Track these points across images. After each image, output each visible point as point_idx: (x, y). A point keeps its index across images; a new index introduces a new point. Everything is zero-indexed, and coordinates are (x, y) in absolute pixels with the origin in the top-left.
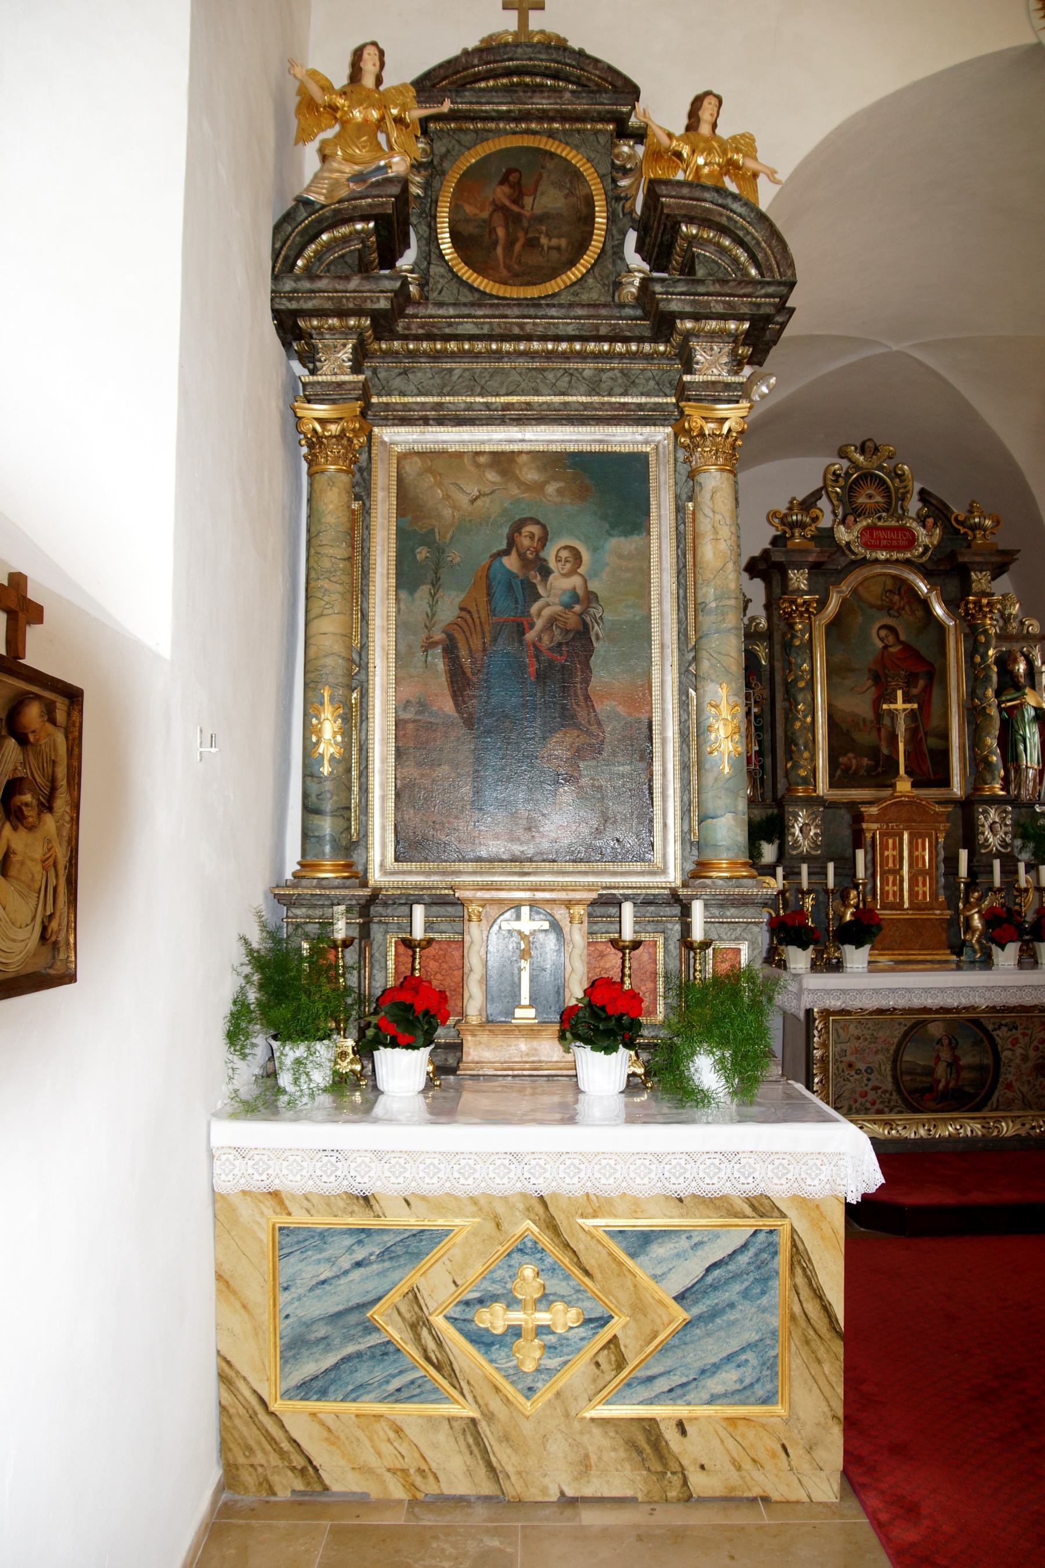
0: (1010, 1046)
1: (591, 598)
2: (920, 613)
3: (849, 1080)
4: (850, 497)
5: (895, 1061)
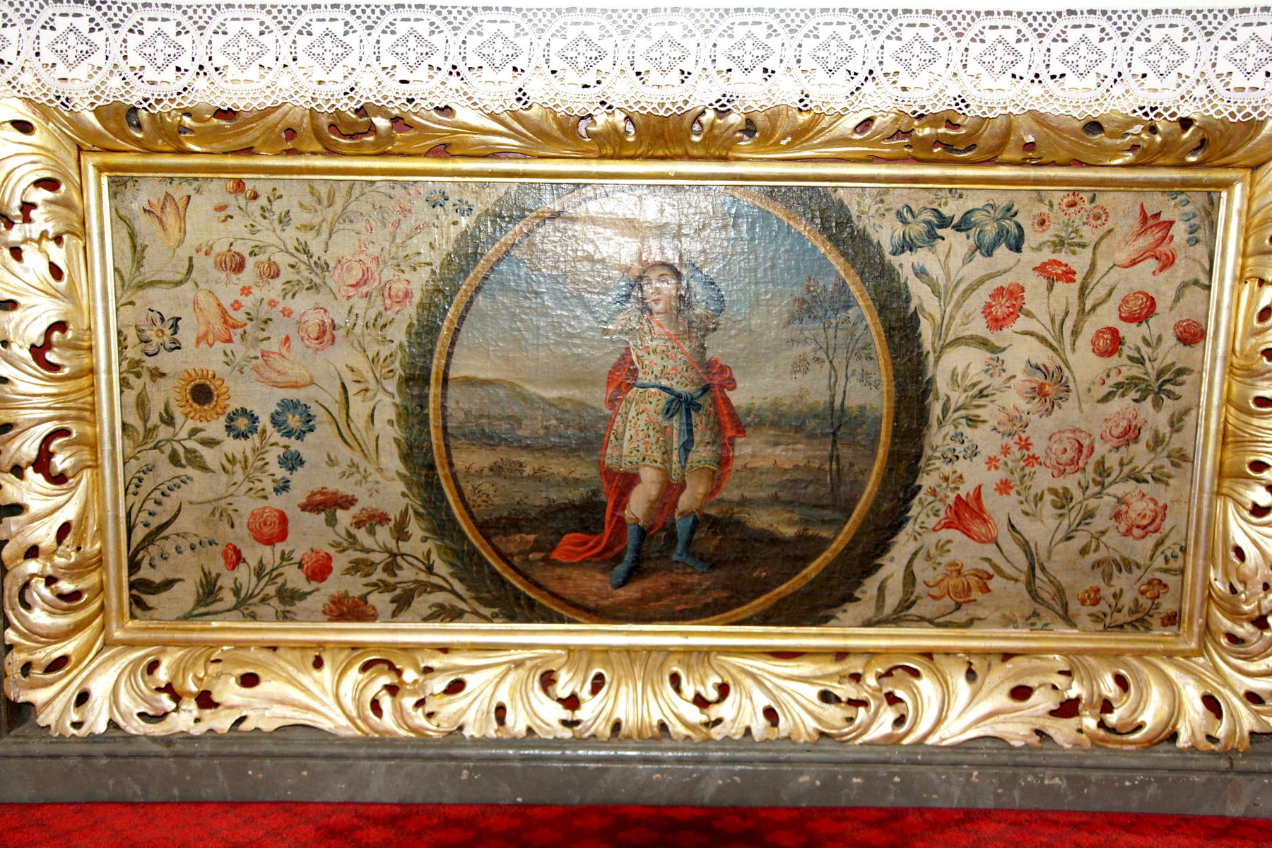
0: (979, 327)
3: (196, 461)
5: (416, 379)
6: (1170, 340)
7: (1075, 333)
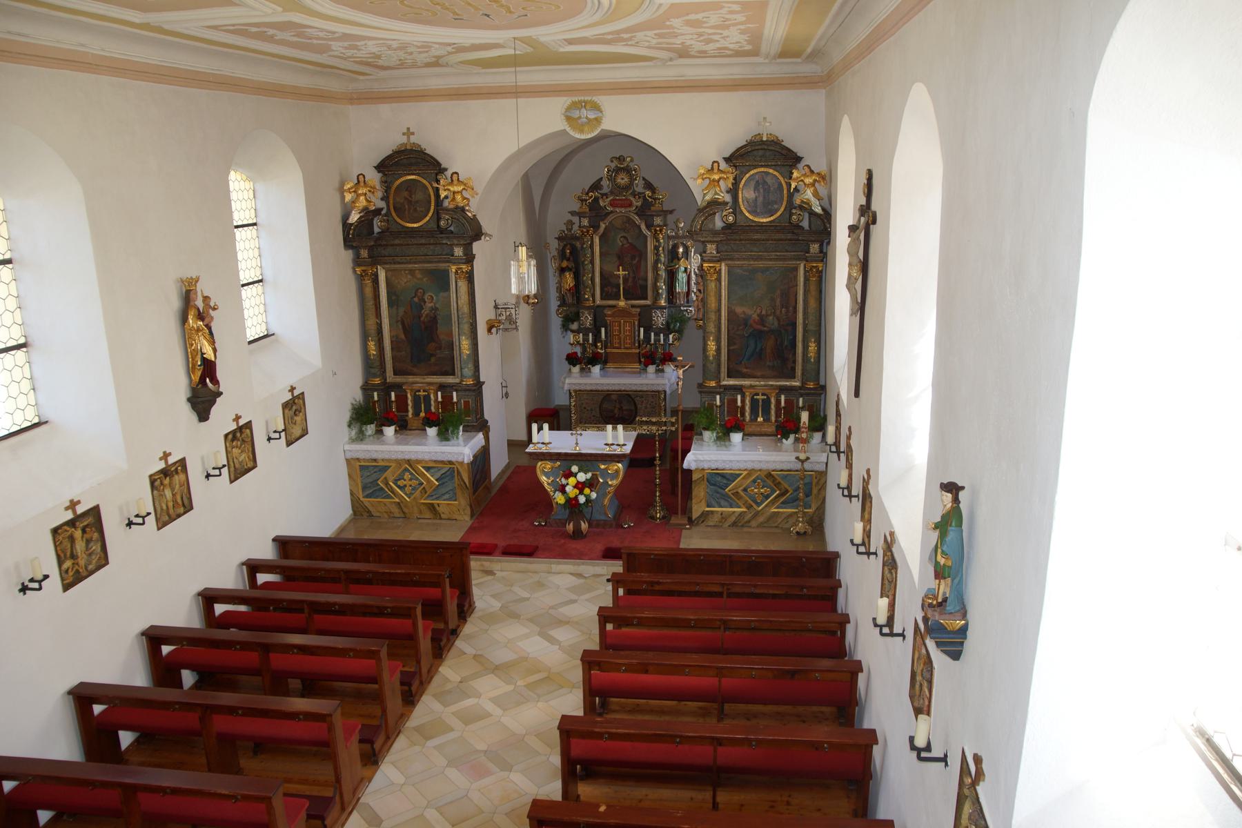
1: (436, 309)
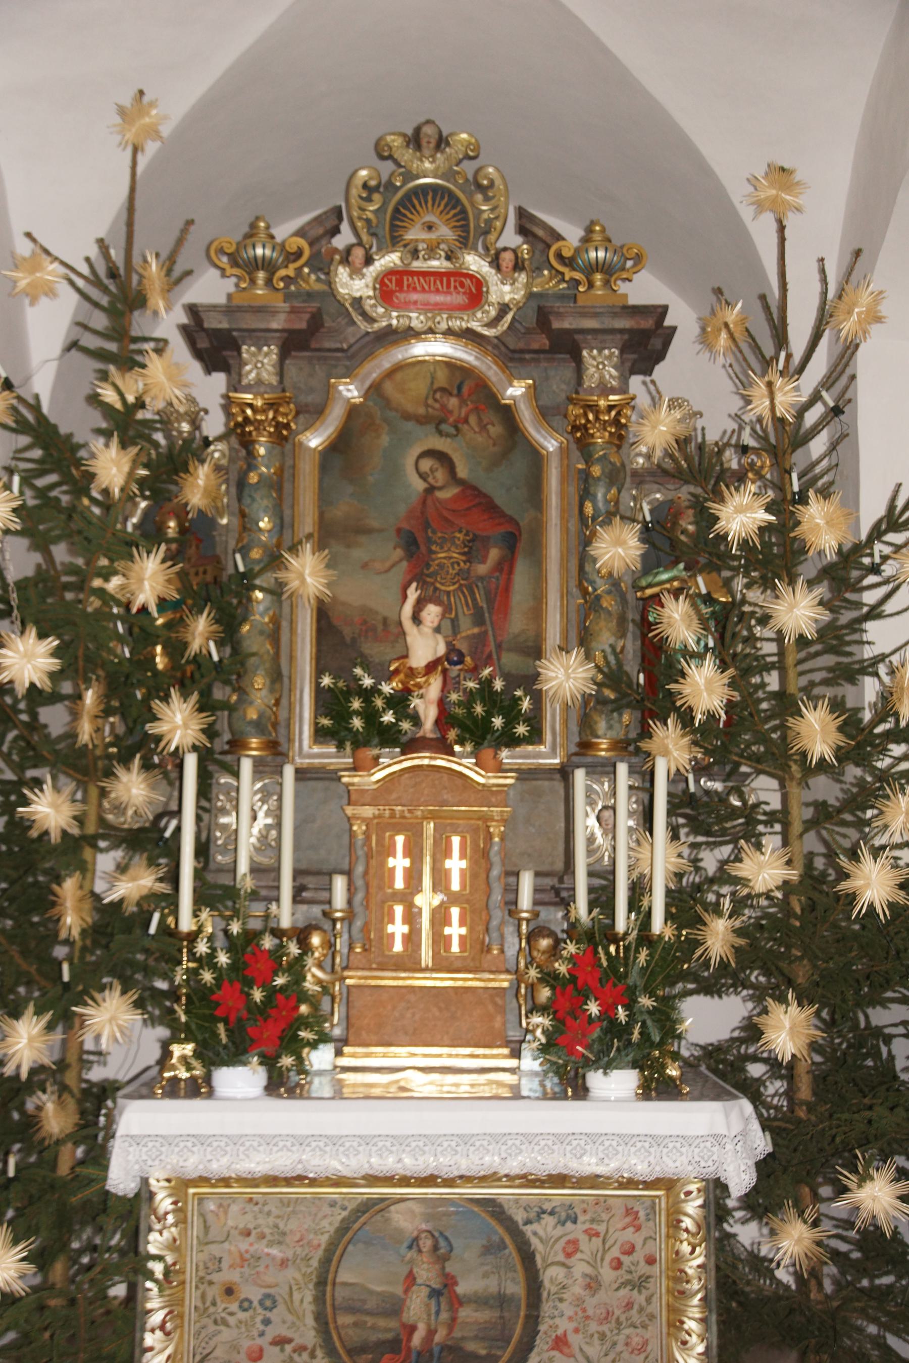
0: (561, 1257)
2: (496, 430)
3: (225, 1323)
4: (393, 227)
5: (321, 1283)
6: (642, 1263)
7: (602, 1260)
